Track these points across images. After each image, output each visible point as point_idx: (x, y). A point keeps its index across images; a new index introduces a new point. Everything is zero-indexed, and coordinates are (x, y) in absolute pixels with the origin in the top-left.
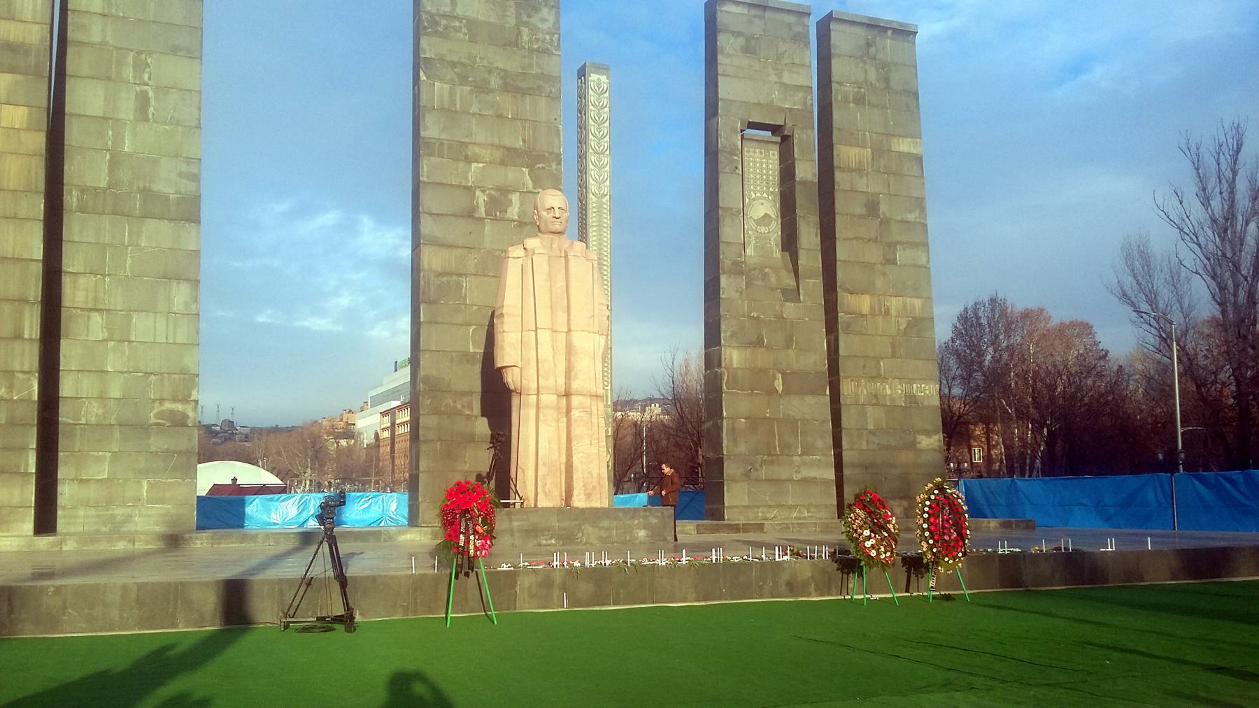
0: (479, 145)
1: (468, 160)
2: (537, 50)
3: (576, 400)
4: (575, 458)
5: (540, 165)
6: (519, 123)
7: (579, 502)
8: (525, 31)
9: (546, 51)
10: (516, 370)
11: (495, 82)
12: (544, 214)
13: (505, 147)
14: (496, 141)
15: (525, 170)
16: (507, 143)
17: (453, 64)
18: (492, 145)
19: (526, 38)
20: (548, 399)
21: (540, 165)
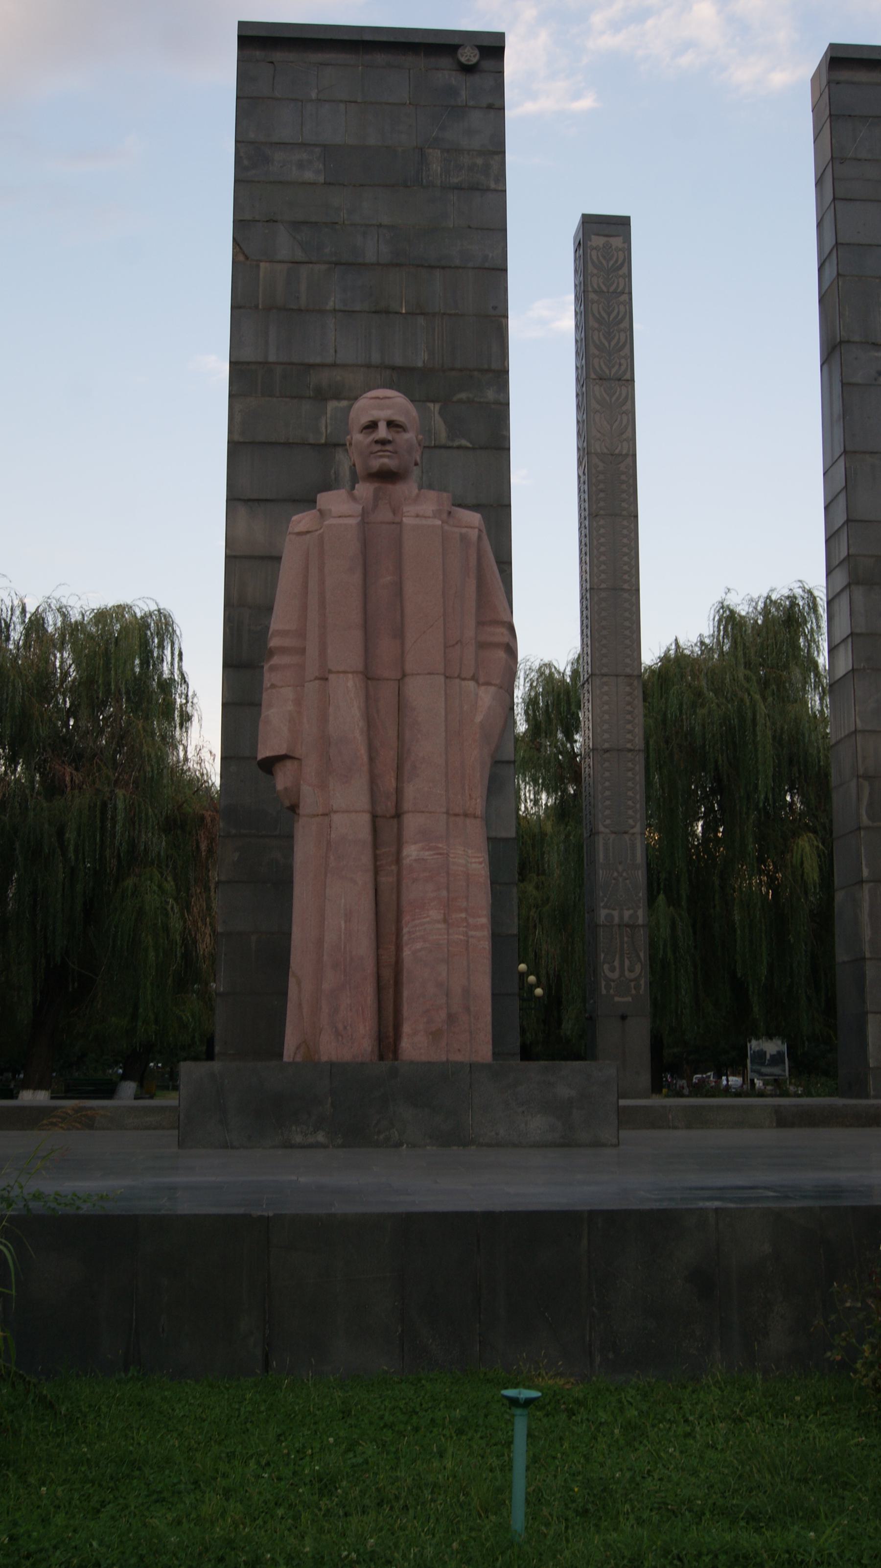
0: (344, 366)
1: (322, 396)
2: (458, 188)
3: (412, 823)
4: (406, 953)
5: (463, 396)
6: (421, 320)
7: (415, 1045)
8: (435, 155)
9: (475, 188)
10: (289, 764)
11: (373, 249)
12: (358, 437)
13: (393, 368)
14: (376, 358)
15: (435, 408)
16: (398, 361)
17: (296, 225)
18: (369, 366)
19: (436, 167)
20: (352, 824)
21: (463, 396)
